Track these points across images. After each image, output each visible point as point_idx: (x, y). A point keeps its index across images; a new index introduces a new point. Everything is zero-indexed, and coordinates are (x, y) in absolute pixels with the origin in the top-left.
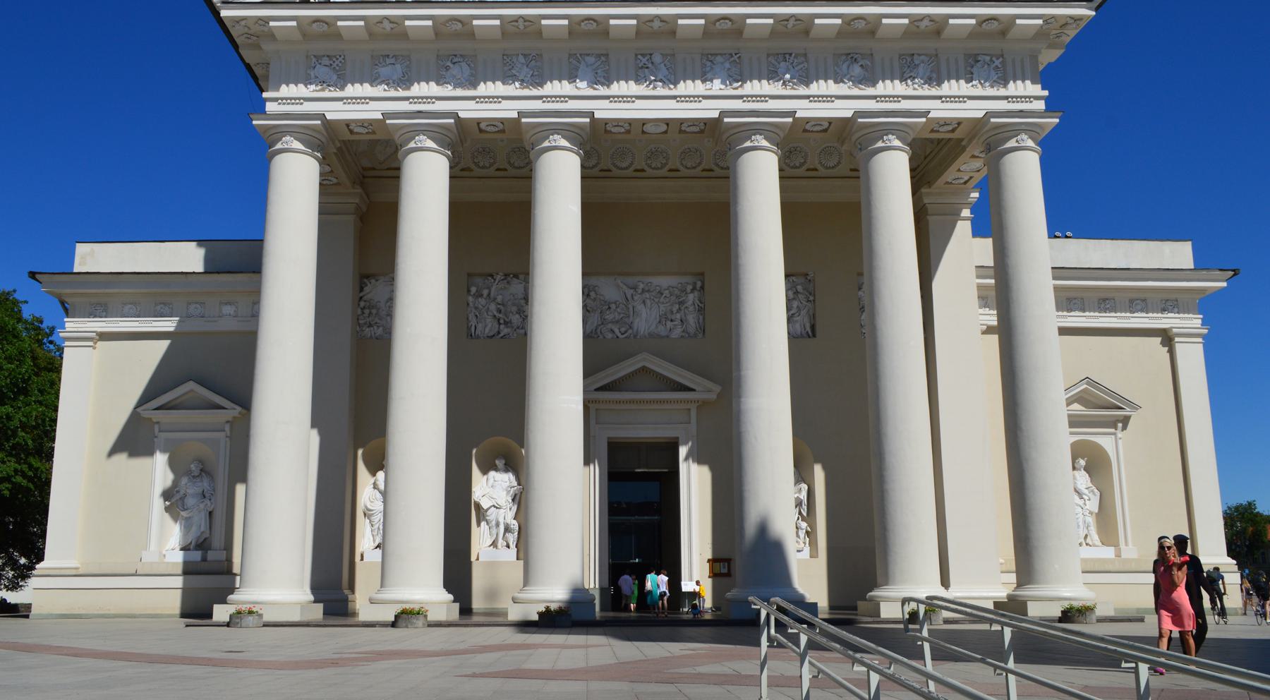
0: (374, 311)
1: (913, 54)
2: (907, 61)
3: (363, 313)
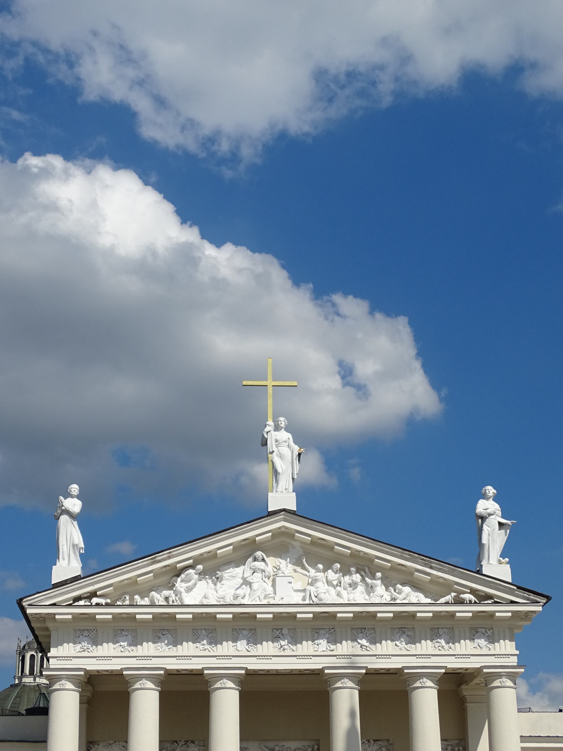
2: (435, 633)
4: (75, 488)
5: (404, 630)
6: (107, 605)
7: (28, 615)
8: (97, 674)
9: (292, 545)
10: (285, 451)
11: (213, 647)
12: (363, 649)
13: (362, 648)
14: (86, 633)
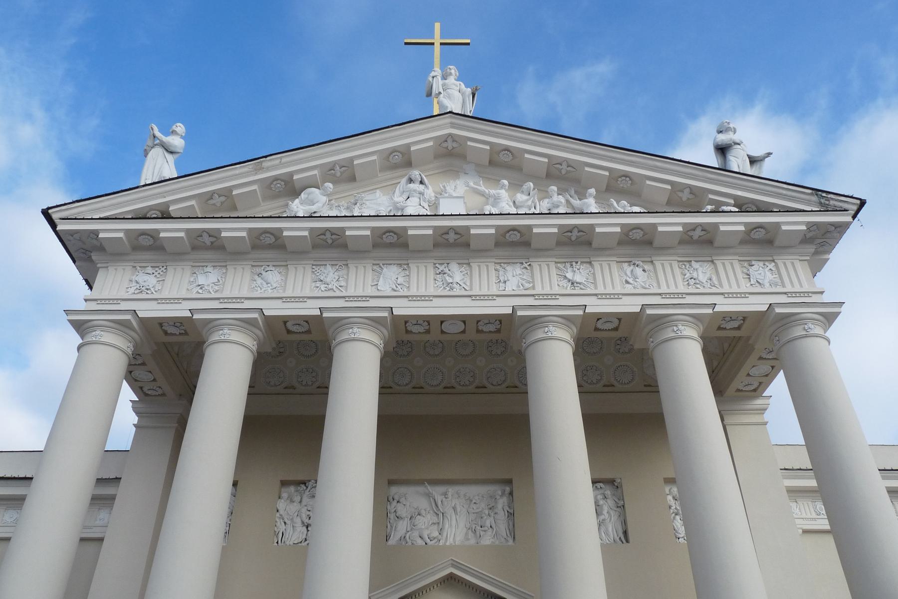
1: (691, 261)
2: (685, 266)
12: (576, 288)
14: (149, 270)
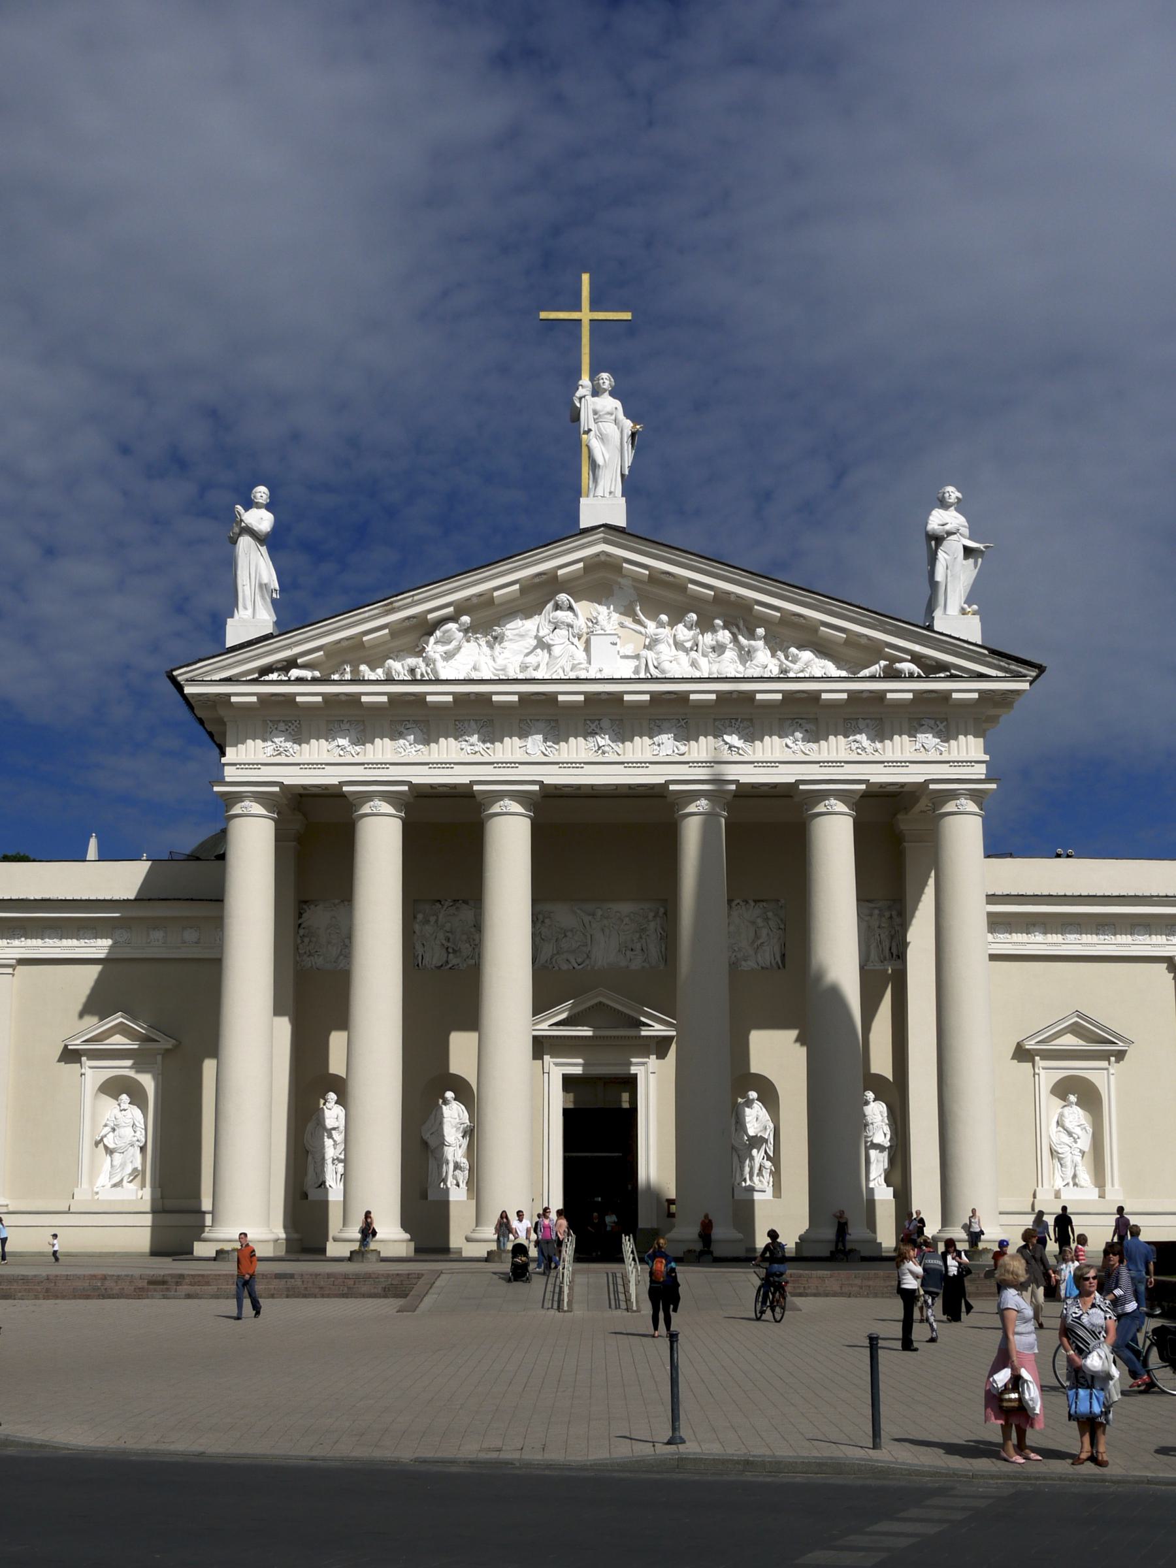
0: (314, 939)
3: (303, 942)
4: (261, 493)
5: (800, 721)
6: (314, 681)
7: (188, 696)
8: (302, 791)
9: (619, 583)
10: (610, 429)
11: (488, 748)
12: (733, 753)
13: (731, 751)
14: (282, 726)
